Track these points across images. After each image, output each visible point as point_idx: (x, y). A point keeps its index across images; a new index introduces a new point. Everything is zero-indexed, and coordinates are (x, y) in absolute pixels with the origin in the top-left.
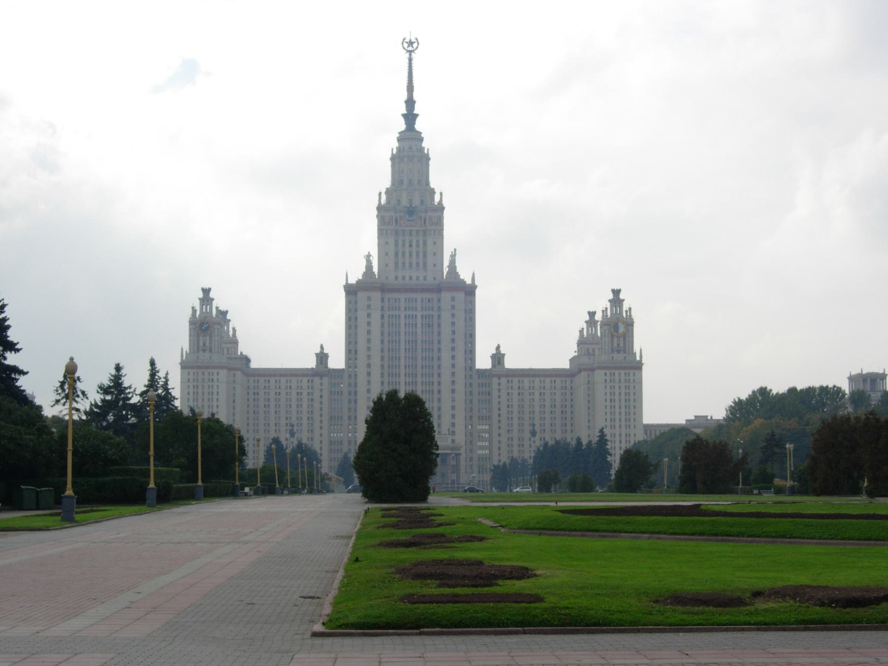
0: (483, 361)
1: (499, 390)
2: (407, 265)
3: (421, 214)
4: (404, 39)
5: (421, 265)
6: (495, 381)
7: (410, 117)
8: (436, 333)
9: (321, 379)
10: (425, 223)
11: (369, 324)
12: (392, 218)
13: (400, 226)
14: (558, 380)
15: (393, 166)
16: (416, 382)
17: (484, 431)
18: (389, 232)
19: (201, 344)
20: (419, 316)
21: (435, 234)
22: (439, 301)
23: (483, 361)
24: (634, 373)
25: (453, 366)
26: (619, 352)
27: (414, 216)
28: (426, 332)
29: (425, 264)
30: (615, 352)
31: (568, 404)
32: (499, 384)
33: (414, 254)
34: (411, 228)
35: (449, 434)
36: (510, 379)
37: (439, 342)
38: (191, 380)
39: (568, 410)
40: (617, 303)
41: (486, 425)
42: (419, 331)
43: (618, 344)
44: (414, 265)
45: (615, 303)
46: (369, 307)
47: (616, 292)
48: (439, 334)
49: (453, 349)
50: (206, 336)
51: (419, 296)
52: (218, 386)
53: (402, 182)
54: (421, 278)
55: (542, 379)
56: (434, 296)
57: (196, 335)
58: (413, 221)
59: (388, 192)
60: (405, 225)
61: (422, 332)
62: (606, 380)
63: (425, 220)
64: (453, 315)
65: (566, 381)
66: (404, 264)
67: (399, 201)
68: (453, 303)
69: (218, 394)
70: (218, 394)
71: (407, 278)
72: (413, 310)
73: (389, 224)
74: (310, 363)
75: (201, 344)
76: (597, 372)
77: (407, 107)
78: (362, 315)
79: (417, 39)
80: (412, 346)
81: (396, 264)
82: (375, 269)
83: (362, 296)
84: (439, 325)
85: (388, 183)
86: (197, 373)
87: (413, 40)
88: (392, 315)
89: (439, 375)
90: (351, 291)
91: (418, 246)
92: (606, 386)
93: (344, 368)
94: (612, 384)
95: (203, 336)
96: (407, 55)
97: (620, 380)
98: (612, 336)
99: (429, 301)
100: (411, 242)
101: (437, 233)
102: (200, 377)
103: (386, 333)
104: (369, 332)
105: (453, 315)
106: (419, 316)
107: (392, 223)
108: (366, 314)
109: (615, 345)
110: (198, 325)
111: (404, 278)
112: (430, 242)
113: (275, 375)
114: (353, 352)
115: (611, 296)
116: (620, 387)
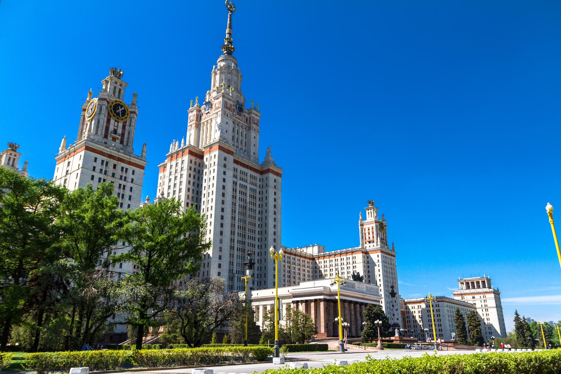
3: (245, 114)
10: (247, 122)
14: (307, 260)
38: (97, 169)
42: (248, 200)
50: (118, 122)
51: (249, 172)
52: (131, 188)
56: (257, 175)
58: (241, 116)
60: (236, 116)
63: (247, 119)
69: (130, 199)
70: (130, 199)
86: (107, 163)
95: (116, 121)
102: (110, 170)
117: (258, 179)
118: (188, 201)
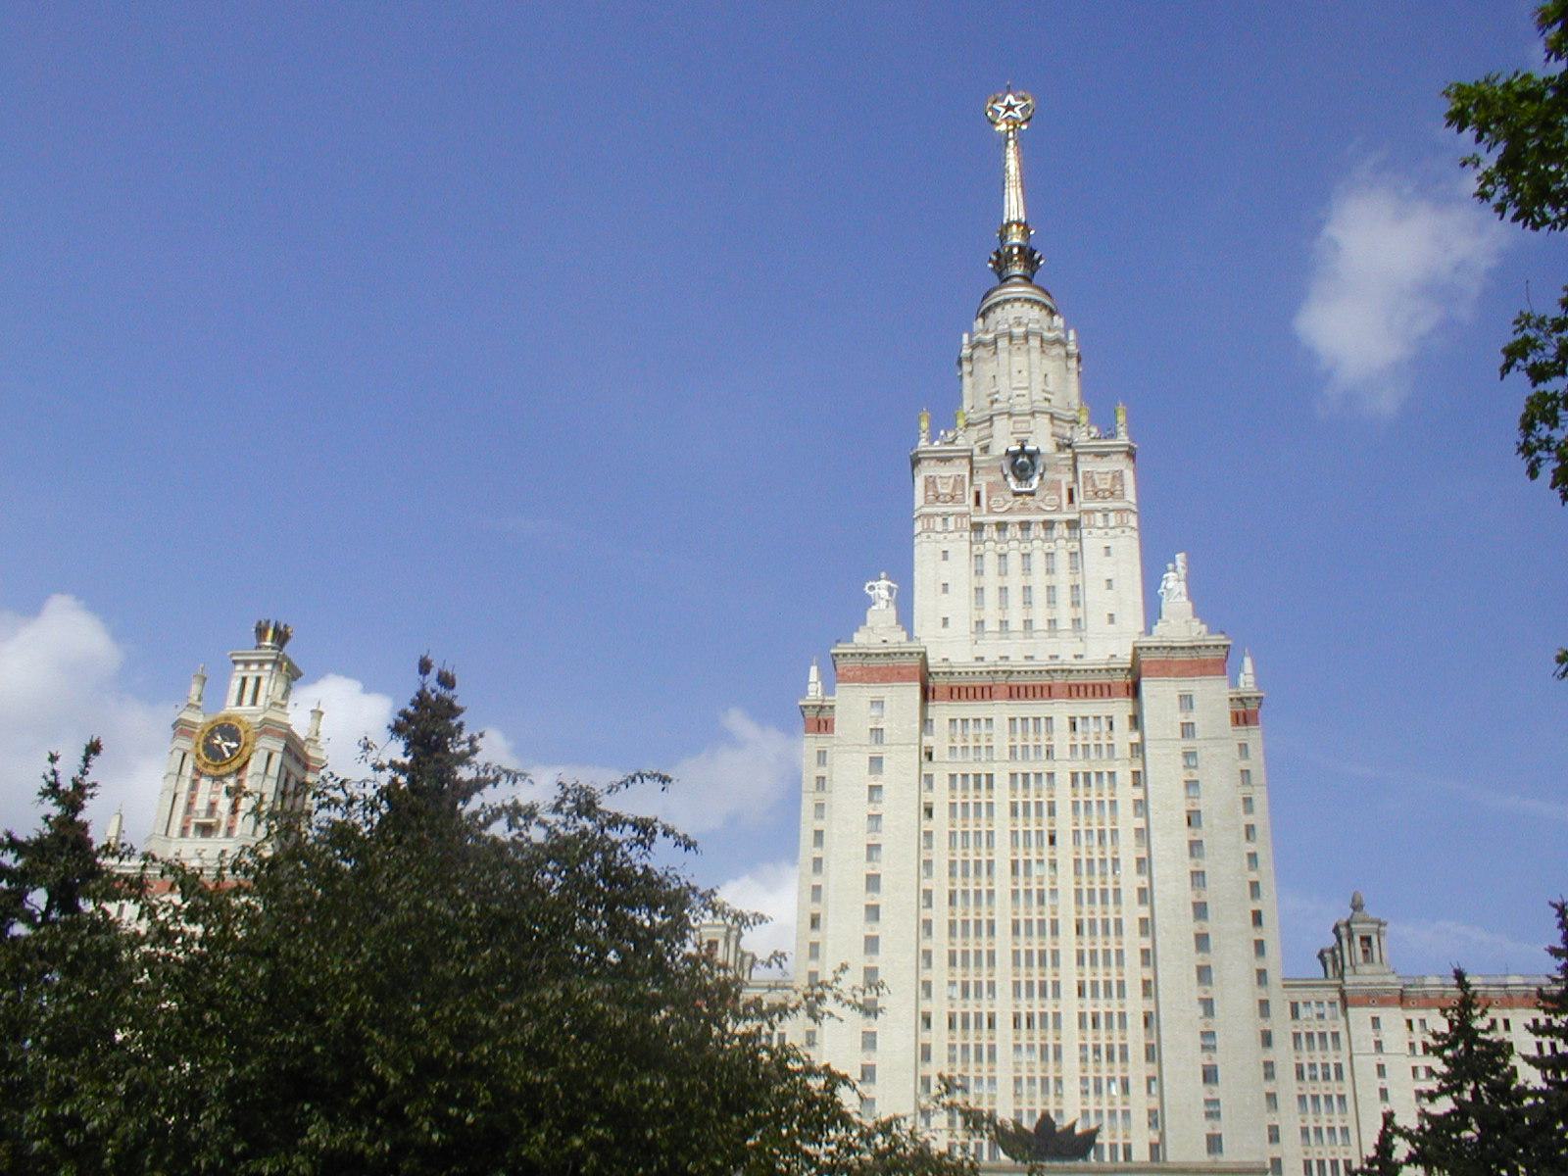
3: (1058, 477)
5: (1065, 623)
6: (1360, 1015)
12: (963, 481)
13: (990, 511)
18: (951, 519)
19: (201, 804)
20: (1063, 778)
22: (1136, 721)
27: (1035, 481)
33: (1039, 595)
51: (1061, 711)
60: (1006, 508)
67: (985, 449)
75: (201, 804)
101: (1112, 524)
106: (1063, 778)
107: (963, 494)
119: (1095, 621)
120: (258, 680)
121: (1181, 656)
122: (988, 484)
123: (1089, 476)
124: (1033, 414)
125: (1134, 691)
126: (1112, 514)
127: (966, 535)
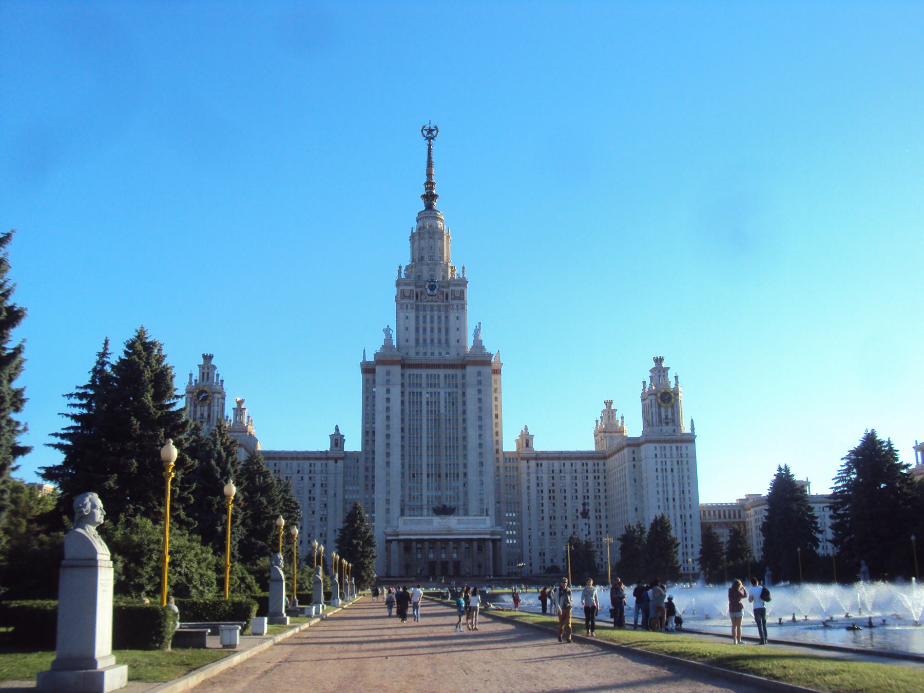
0: (509, 445)
1: (528, 474)
2: (428, 341)
3: (443, 289)
4: (424, 127)
5: (443, 341)
6: (524, 464)
7: (429, 198)
8: (460, 410)
9: (336, 462)
11: (388, 400)
13: (421, 301)
14: (590, 463)
15: (413, 243)
16: (439, 465)
17: (512, 519)
18: (409, 306)
19: (198, 414)
21: (458, 309)
22: (464, 377)
23: (509, 445)
24: (687, 447)
25: (480, 445)
26: (667, 423)
27: (435, 291)
28: (449, 411)
29: (447, 341)
30: (664, 424)
31: (602, 488)
32: (528, 467)
34: (432, 303)
35: (487, 515)
36: (539, 462)
37: (464, 420)
39: (602, 494)
40: (662, 371)
41: (514, 512)
42: (442, 410)
43: (667, 417)
44: (436, 341)
45: (659, 372)
46: (388, 381)
47: (659, 361)
48: (464, 412)
49: (480, 427)
50: (204, 406)
51: (442, 372)
53: (422, 259)
54: (444, 353)
55: (574, 462)
56: (458, 372)
57: (193, 405)
58: (434, 295)
59: (407, 268)
61: (446, 410)
62: (656, 455)
63: (447, 295)
64: (480, 391)
65: (598, 463)
66: (425, 340)
67: (419, 277)
68: (479, 378)
71: (429, 354)
72: (435, 387)
73: (410, 298)
74: (325, 445)
75: (198, 414)
76: (642, 447)
77: (426, 189)
78: (380, 391)
79: (436, 127)
80: (435, 426)
81: (417, 341)
82: (395, 343)
83: (379, 369)
84: (464, 403)
85: (409, 263)
87: (433, 128)
88: (413, 393)
89: (465, 456)
90: (368, 370)
91: (439, 322)
92: (656, 461)
93: (360, 450)
94: (664, 460)
95: (201, 406)
96: (427, 141)
97: (671, 454)
98: (659, 406)
99: (453, 378)
100: (432, 317)
101: (459, 308)
103: (407, 411)
104: (388, 409)
105: (480, 391)
108: (385, 390)
109: (663, 416)
110: (195, 394)
111: (425, 353)
112: (452, 316)
113: (286, 459)
114: (370, 433)
115: (653, 365)
116: (672, 461)
117: (460, 376)
118: (367, 430)
119: (453, 342)
120: (208, 373)
121: (479, 359)
122: (421, 291)
123: (453, 291)
124: (436, 265)
125: (463, 366)
126: (459, 306)
127: (414, 311)
